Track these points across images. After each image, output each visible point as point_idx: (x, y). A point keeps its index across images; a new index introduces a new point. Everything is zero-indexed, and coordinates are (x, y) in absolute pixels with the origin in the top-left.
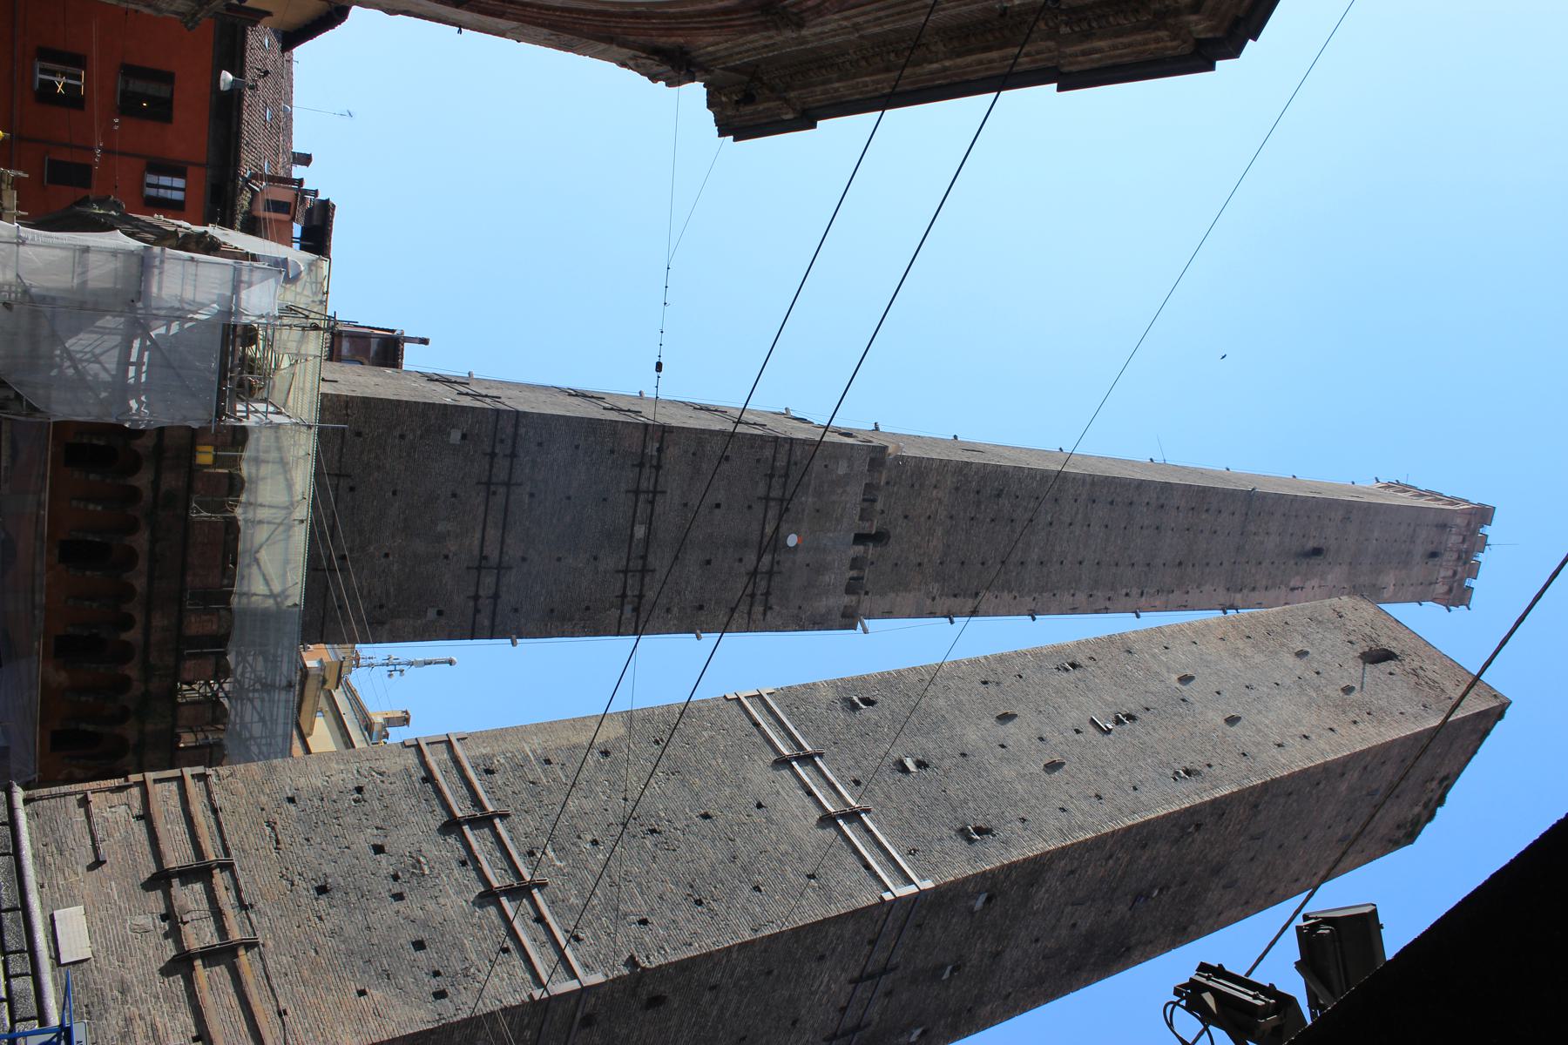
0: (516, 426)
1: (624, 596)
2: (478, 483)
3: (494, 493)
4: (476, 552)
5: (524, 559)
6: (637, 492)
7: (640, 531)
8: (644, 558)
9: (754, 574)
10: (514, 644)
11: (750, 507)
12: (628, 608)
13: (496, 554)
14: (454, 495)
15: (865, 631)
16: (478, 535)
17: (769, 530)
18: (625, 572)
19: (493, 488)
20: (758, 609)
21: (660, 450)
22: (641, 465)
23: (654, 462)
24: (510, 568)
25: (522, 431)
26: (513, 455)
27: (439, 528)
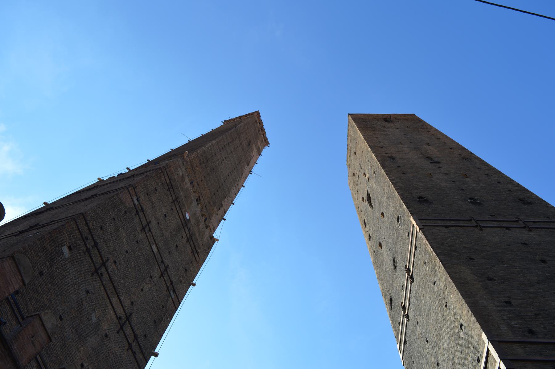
0: (87, 224)
1: (168, 287)
2: (92, 275)
3: (102, 274)
4: (115, 319)
5: (132, 303)
6: (143, 229)
7: (154, 248)
8: (162, 262)
9: (188, 241)
10: (156, 355)
11: (172, 209)
12: (171, 292)
13: (122, 311)
14: (88, 292)
15: (218, 240)
16: (110, 307)
17: (181, 217)
18: (162, 275)
19: (99, 272)
20: (196, 255)
21: (137, 200)
22: (137, 213)
23: (140, 208)
24: (131, 314)
25: (90, 224)
26: (96, 245)
27: (94, 319)
